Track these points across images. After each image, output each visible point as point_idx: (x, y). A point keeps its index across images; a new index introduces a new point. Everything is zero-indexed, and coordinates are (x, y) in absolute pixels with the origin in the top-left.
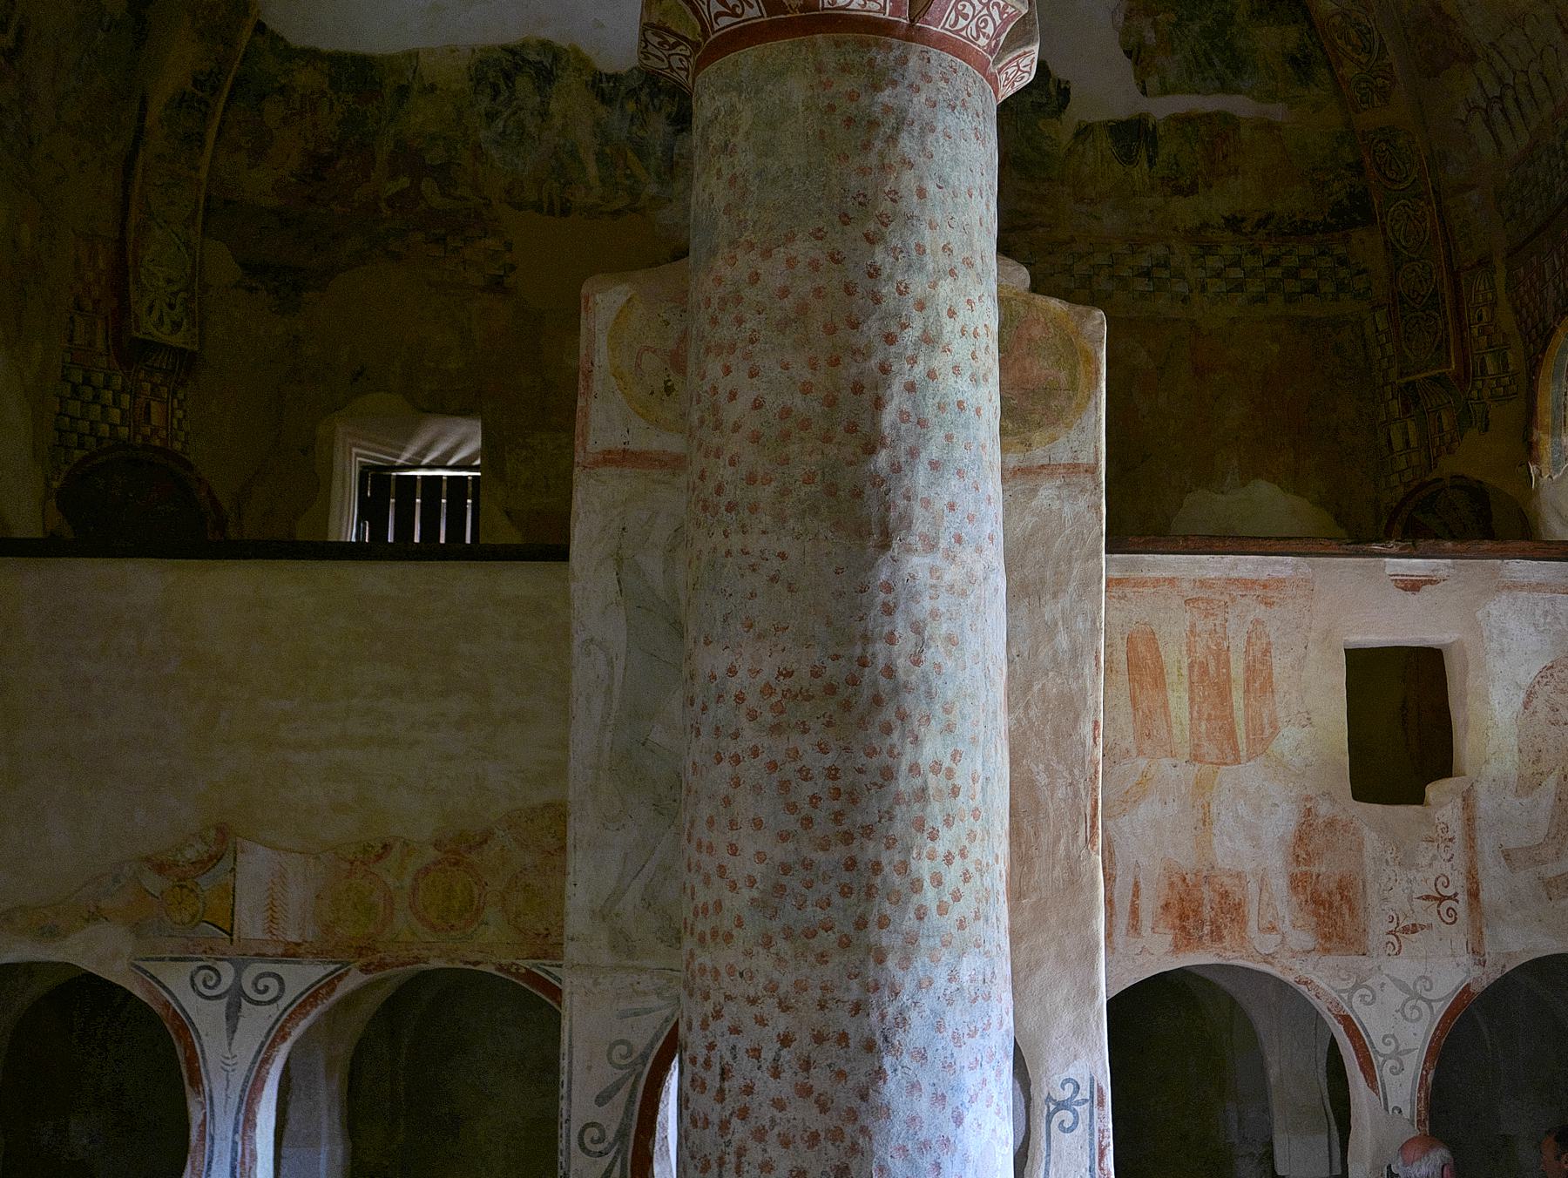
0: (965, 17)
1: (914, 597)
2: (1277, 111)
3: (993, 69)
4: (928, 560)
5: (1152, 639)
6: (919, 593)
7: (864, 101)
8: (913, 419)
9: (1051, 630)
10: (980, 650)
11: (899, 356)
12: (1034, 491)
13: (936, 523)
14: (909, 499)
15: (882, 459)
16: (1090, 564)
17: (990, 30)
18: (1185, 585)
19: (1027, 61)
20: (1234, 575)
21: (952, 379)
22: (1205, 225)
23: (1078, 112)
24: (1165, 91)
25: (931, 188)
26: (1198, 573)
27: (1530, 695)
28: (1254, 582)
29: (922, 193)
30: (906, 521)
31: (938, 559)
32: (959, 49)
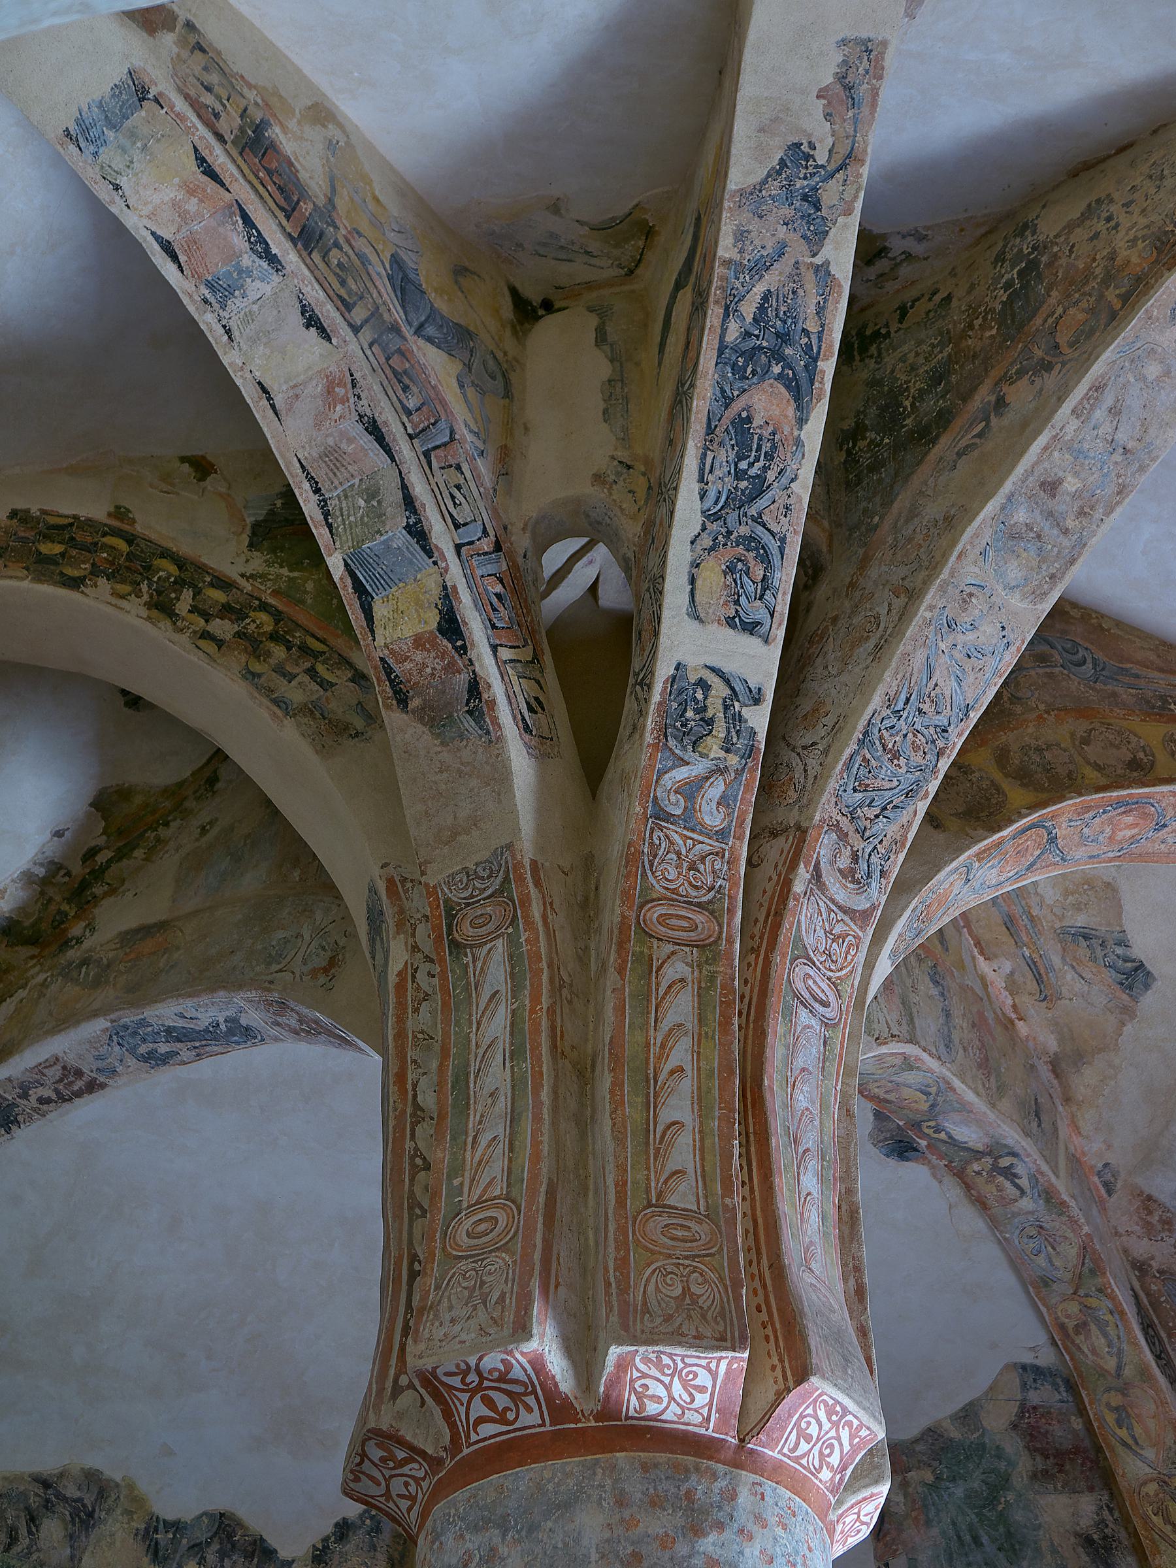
3: (833, 1516)
7: (682, 1549)
17: (835, 1460)
32: (799, 1485)
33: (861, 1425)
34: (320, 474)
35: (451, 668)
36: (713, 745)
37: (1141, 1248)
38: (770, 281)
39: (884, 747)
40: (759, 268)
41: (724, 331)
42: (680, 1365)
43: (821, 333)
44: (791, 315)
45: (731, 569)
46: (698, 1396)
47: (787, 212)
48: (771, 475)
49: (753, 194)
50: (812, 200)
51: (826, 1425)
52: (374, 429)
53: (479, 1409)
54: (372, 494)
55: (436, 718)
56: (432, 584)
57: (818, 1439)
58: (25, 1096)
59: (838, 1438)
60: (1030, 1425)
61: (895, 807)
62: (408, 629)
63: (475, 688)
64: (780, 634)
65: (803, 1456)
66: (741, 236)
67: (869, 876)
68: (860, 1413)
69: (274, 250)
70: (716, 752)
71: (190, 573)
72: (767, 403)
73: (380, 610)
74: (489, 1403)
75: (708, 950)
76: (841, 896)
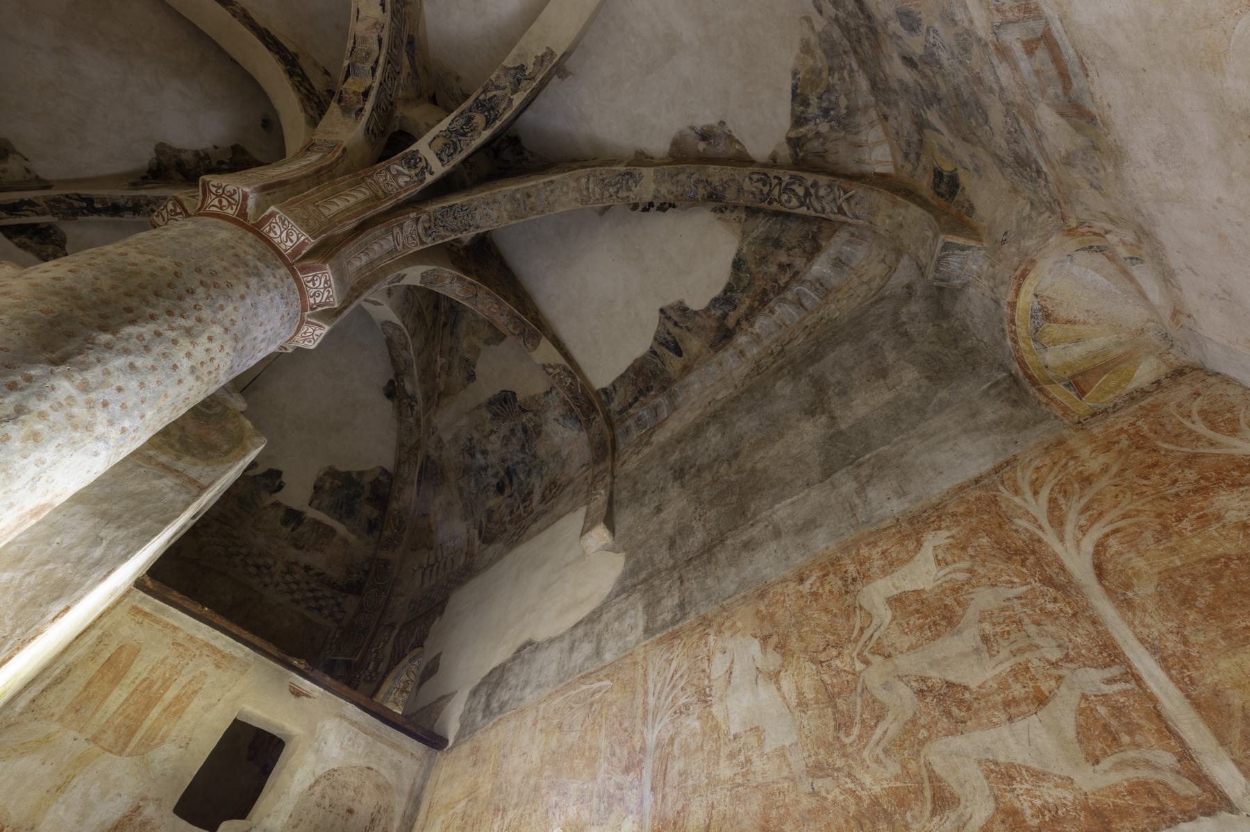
1: (40, 396)
2: (352, 538)
4: (74, 392)
5: (135, 653)
6: (46, 398)
8: (145, 343)
9: (98, 540)
10: (48, 463)
11: (166, 321)
12: (161, 477)
13: (102, 385)
14: (99, 361)
15: (105, 337)
16: (157, 526)
17: (318, 300)
18: (181, 635)
19: (318, 332)
20: (212, 642)
21: (182, 354)
22: (296, 563)
23: (279, 497)
24: (318, 508)
25: (248, 301)
26: (193, 632)
27: (317, 782)
28: (220, 652)
29: (243, 297)
30: (84, 367)
31: (81, 398)
32: (303, 294)
34: (358, 41)
35: (358, 102)
36: (413, 173)
37: (432, 452)
40: (498, 88)
44: (498, 105)
49: (507, 69)
50: (519, 81)
52: (380, 41)
53: (216, 202)
54: (368, 54)
55: (346, 110)
56: (368, 83)
58: (147, 205)
60: (376, 484)
62: (354, 88)
63: (361, 110)
64: (447, 168)
66: (498, 77)
70: (413, 173)
71: (304, 77)
72: (479, 119)
73: (350, 80)
74: (220, 202)
75: (376, 199)
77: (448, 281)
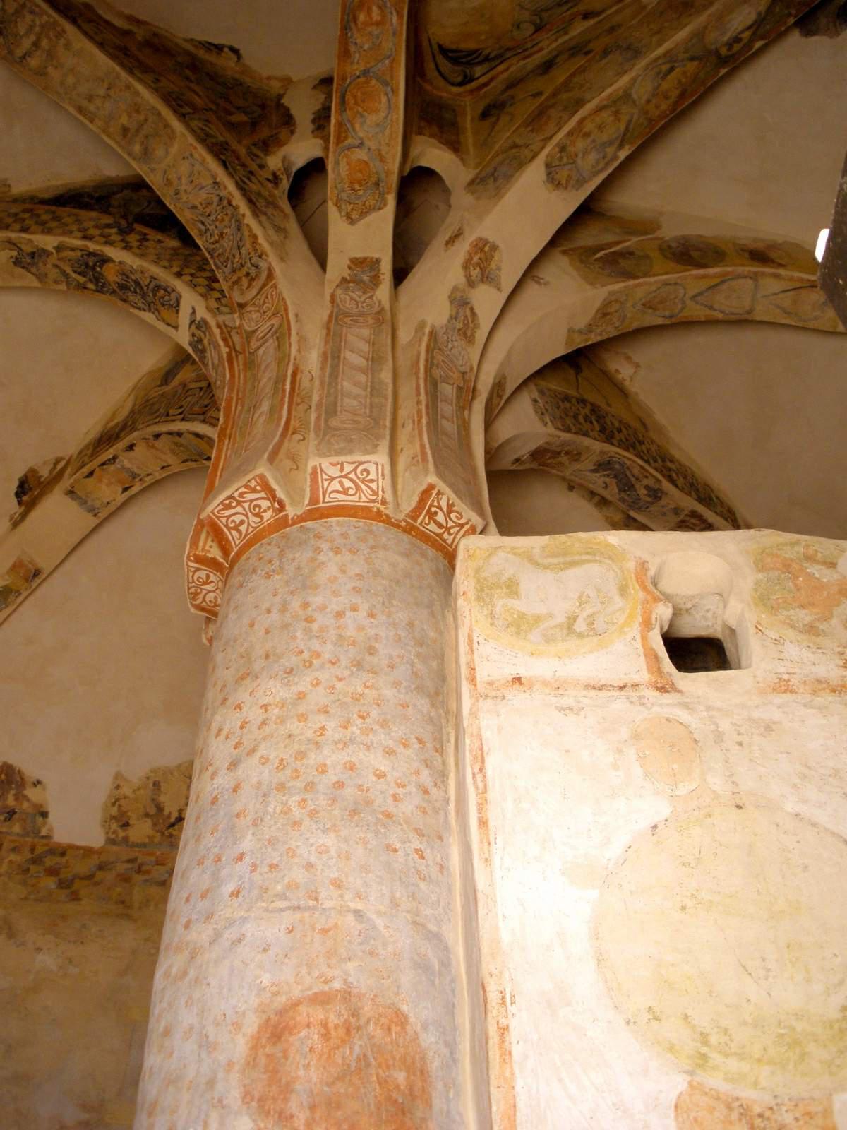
0: (242, 522)
33: (246, 486)
38: (69, 270)
39: (217, 242)
40: (66, 275)
41: (92, 290)
42: (193, 584)
43: (81, 250)
45: (163, 305)
46: (211, 579)
47: (41, 264)
48: (133, 278)
50: (32, 255)
51: (239, 509)
57: (246, 516)
59: (251, 501)
61: (241, 240)
64: (179, 285)
65: (247, 530)
67: (257, 267)
68: (235, 487)
69: (111, 456)
76: (254, 292)
77: (361, 155)
